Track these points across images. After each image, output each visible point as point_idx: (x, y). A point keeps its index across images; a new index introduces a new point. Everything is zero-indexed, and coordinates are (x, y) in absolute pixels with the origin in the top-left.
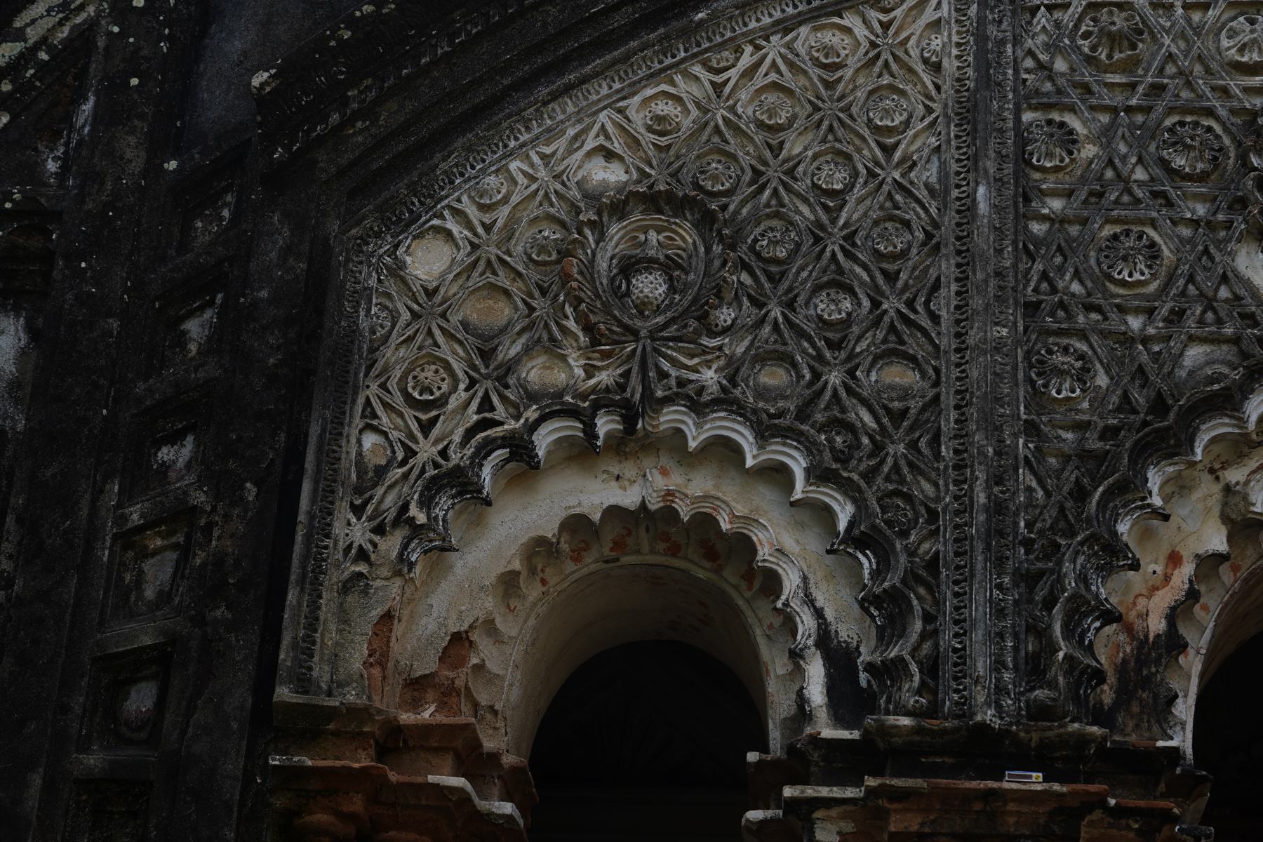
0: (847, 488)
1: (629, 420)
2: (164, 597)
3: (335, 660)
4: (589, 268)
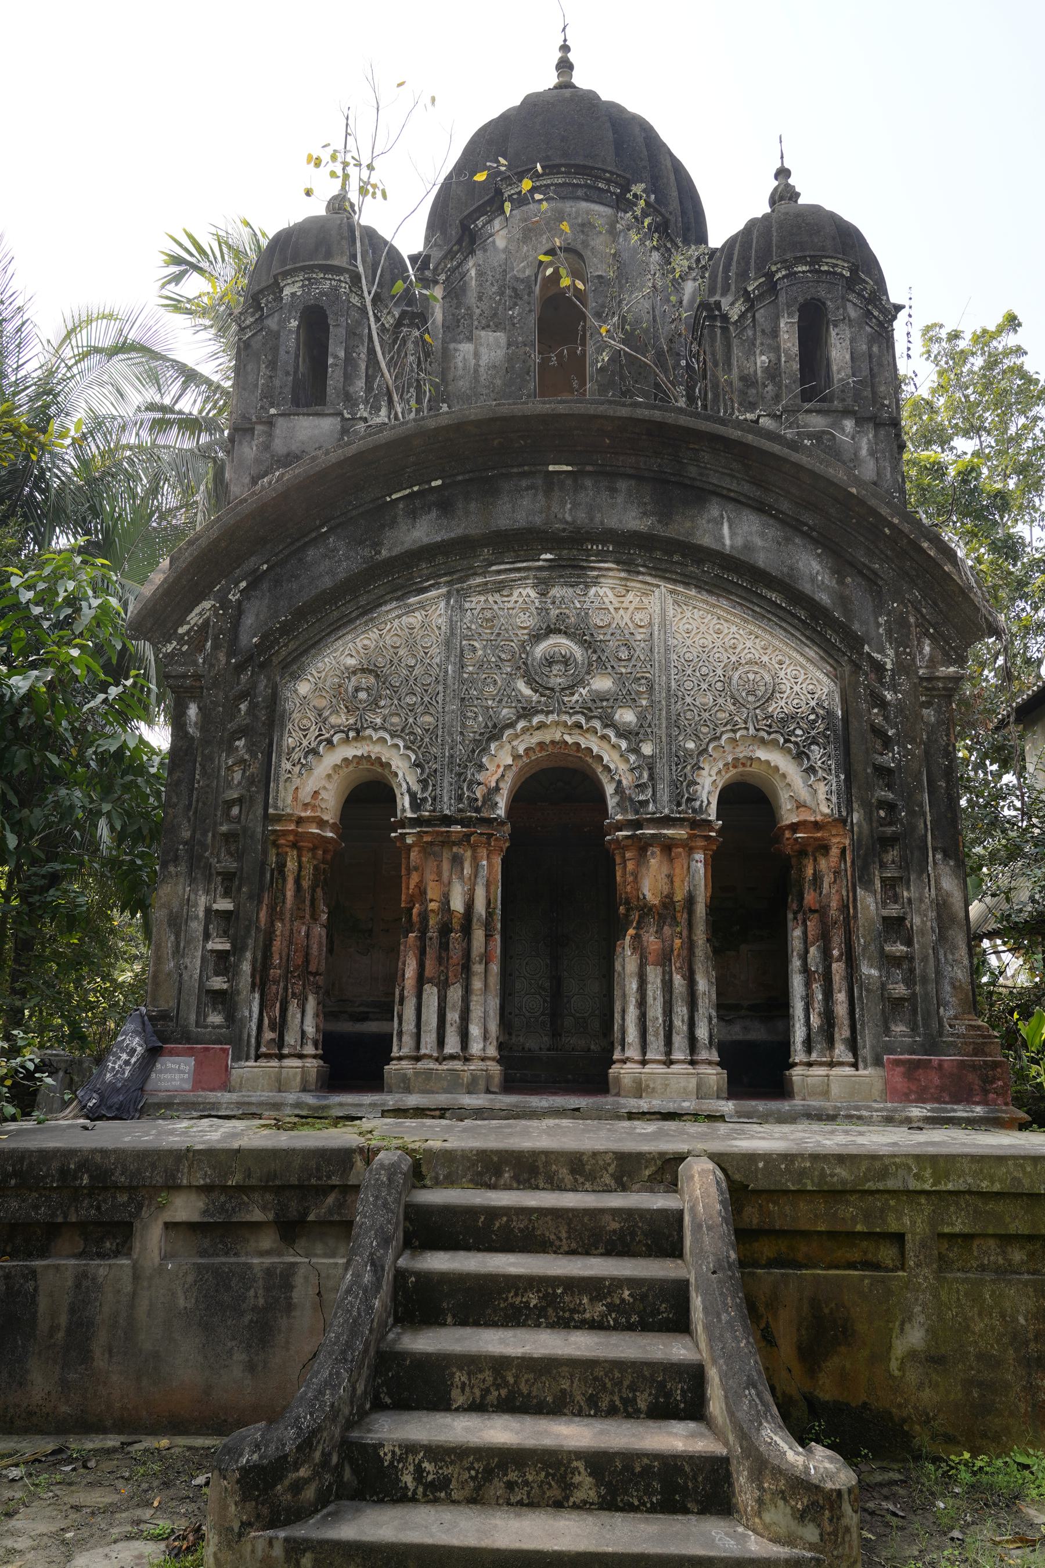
0: (413, 751)
1: (358, 733)
2: (240, 783)
3: (284, 801)
4: (346, 691)
